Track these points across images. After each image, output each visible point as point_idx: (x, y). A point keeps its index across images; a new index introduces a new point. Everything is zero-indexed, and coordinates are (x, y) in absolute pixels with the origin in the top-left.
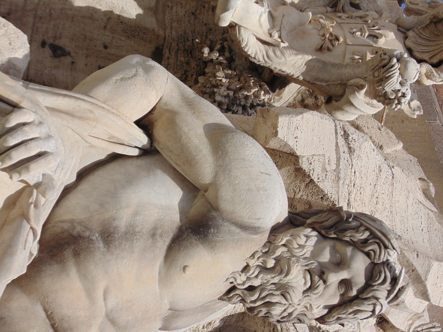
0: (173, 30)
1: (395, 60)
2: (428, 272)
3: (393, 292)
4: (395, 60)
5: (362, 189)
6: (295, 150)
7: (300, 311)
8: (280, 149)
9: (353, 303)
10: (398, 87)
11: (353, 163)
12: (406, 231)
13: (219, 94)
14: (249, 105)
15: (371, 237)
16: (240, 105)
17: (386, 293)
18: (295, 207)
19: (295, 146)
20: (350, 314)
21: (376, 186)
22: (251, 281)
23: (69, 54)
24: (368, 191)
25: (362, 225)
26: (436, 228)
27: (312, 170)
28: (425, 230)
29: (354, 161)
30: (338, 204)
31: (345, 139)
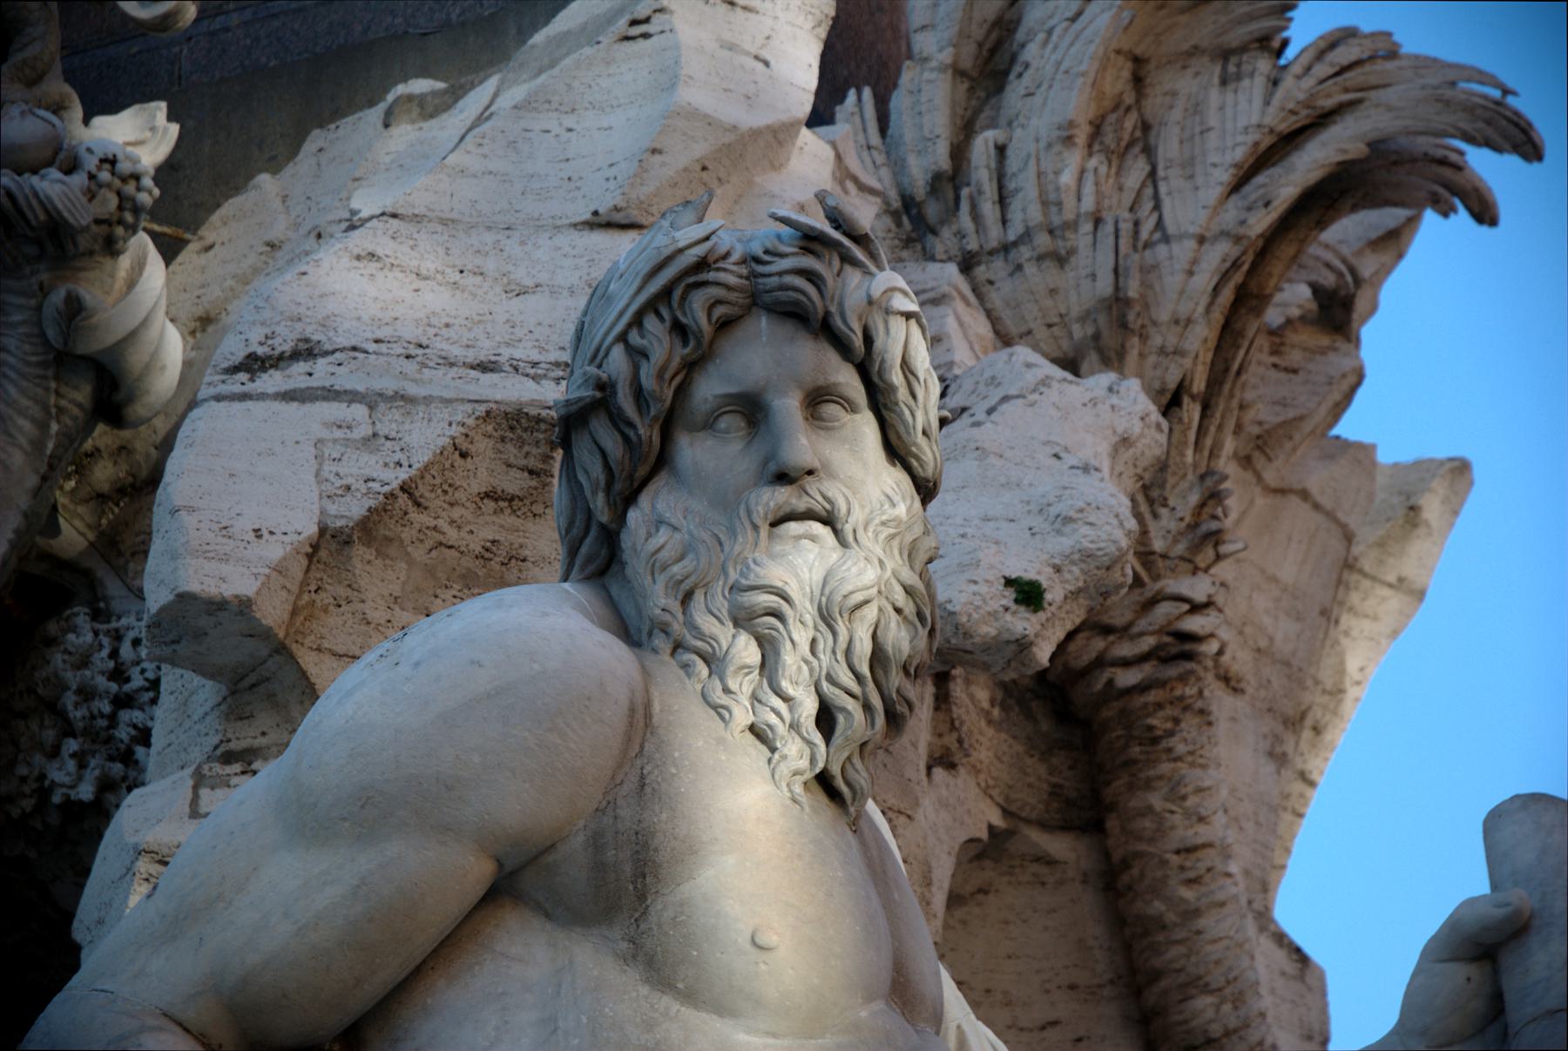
2: (710, 122)
3: (848, 249)
5: (434, 321)
6: (301, 538)
7: (900, 562)
8: (295, 588)
9: (881, 384)
11: (348, 344)
12: (572, 185)
13: (72, 787)
14: (114, 687)
15: (665, 313)
16: (113, 719)
17: (853, 277)
18: (488, 544)
20: (914, 396)
21: (424, 272)
22: (802, 720)
25: (623, 338)
27: (371, 484)
28: (569, 121)
29: (342, 341)
30: (485, 405)
31: (264, 369)
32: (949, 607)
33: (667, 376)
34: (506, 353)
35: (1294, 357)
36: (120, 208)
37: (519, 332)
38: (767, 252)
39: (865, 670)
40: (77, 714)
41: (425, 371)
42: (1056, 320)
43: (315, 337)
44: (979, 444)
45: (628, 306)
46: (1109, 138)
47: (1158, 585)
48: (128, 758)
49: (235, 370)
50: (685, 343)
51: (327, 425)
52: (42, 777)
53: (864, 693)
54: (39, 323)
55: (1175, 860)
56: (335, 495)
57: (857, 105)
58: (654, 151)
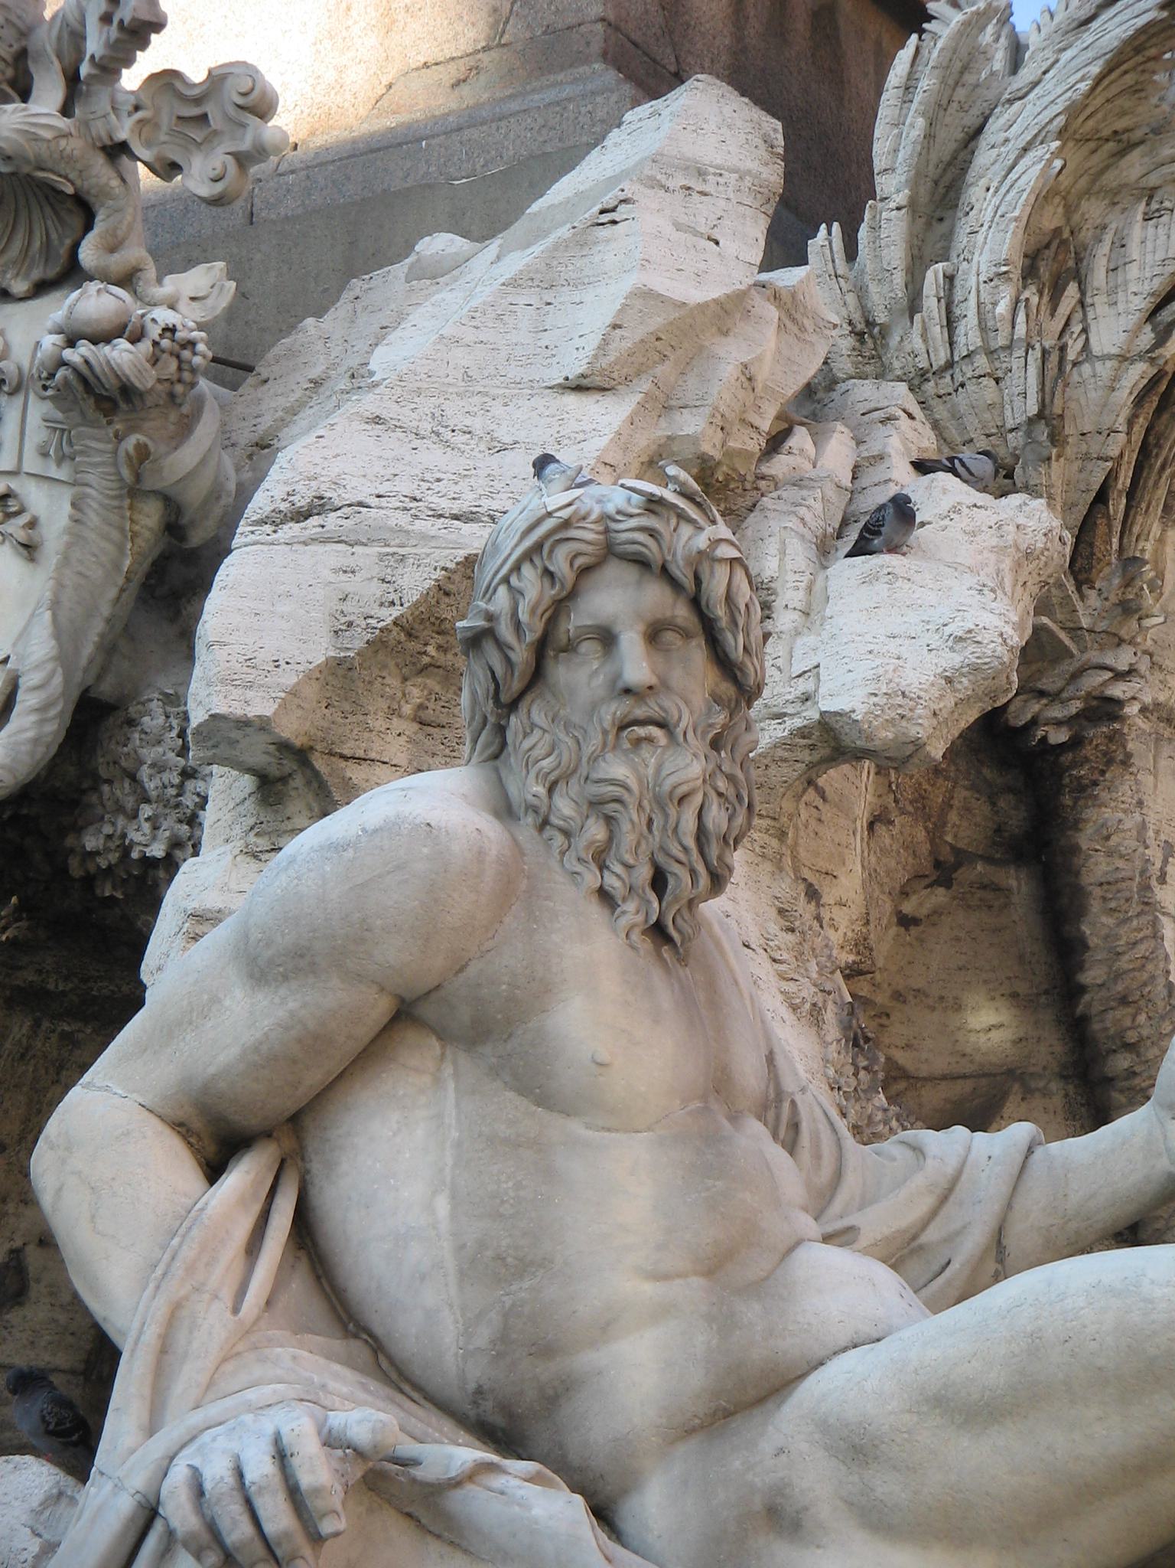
1: (69, 354)
4: (69, 354)
5: (428, 476)
6: (311, 667)
10: (145, 346)
11: (354, 499)
12: (549, 352)
13: (146, 846)
14: (181, 761)
15: (537, 561)
16: (181, 787)
17: (686, 530)
19: (301, 668)
21: (422, 432)
23: (16, 1253)
24: (433, 457)
25: (506, 580)
26: (543, 264)
27: (369, 621)
32: (853, 716)
33: (540, 611)
34: (486, 504)
36: (180, 369)
37: (497, 485)
38: (619, 512)
39: (690, 842)
40: (151, 786)
41: (417, 522)
42: (994, 431)
43: (327, 495)
44: (890, 570)
45: (510, 555)
46: (1045, 271)
47: (1085, 657)
48: (193, 821)
49: (262, 522)
50: (553, 584)
51: (335, 571)
52: (124, 836)
53: (690, 862)
54: (115, 464)
56: (340, 630)
57: (825, 241)
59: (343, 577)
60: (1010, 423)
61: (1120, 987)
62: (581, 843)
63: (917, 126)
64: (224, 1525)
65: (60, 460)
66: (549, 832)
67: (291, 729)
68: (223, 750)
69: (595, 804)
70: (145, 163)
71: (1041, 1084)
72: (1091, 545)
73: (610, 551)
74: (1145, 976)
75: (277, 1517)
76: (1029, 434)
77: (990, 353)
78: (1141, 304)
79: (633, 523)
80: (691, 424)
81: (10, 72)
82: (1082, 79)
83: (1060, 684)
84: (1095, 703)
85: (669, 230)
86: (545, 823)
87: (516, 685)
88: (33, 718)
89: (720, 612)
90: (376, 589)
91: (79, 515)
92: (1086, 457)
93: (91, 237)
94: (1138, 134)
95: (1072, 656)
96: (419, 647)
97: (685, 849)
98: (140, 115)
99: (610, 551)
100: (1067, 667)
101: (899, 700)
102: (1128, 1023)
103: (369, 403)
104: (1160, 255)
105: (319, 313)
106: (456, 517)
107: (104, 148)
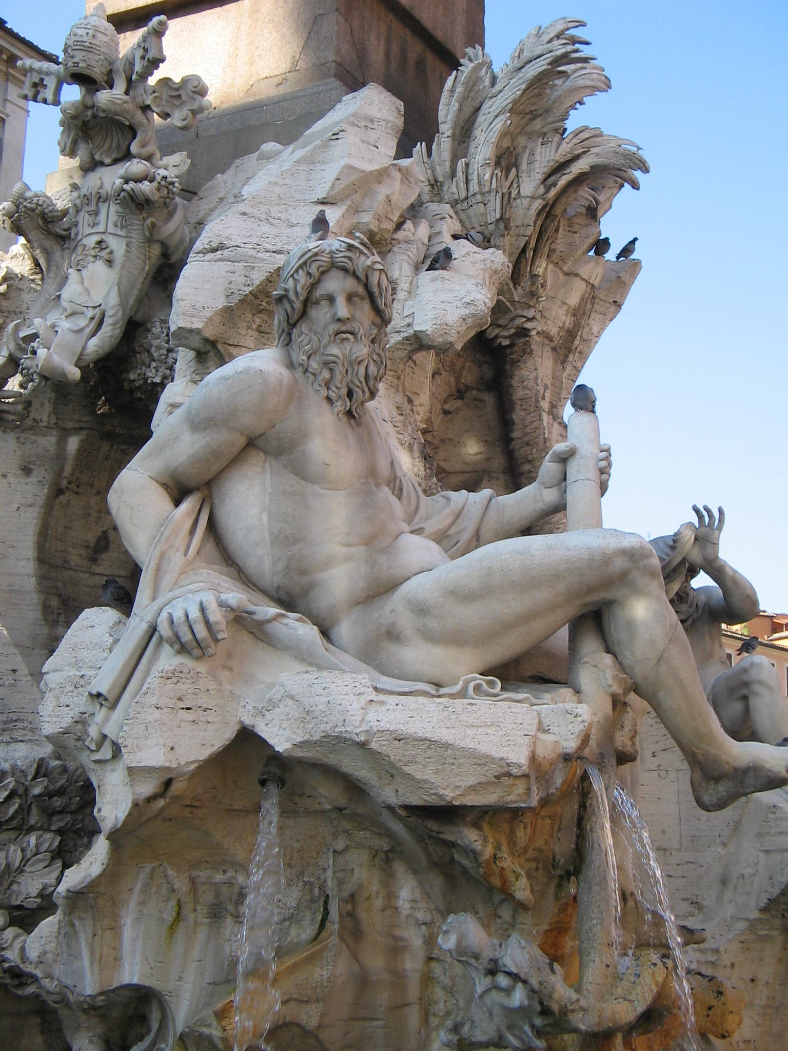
0: (83, 419)
1: (125, 187)
4: (125, 187)
5: (263, 236)
10: (155, 184)
14: (167, 346)
15: (305, 269)
16: (167, 356)
17: (363, 258)
23: (105, 532)
24: (266, 228)
25: (292, 276)
29: (233, 244)
34: (286, 247)
35: (576, 228)
36: (168, 193)
39: (363, 380)
40: (155, 355)
46: (503, 163)
47: (517, 312)
48: (171, 368)
49: (199, 253)
50: (311, 278)
52: (145, 374)
54: (143, 230)
55: (519, 402)
57: (419, 149)
58: (338, 179)
59: (231, 275)
60: (489, 222)
61: (526, 439)
62: (320, 378)
63: (455, 106)
64: (181, 634)
65: (122, 227)
66: (308, 374)
67: (209, 333)
68: (183, 342)
69: (326, 364)
70: (157, 114)
71: (495, 475)
72: (520, 269)
73: (333, 265)
74: (536, 435)
75: (201, 632)
76: (496, 226)
77: (482, 194)
78: (540, 177)
79: (342, 254)
80: (366, 218)
81: (105, 78)
82: (518, 90)
83: (506, 322)
84: (519, 330)
85: (359, 143)
86: (306, 371)
87: (296, 317)
88: (111, 328)
89: (376, 290)
90: (243, 279)
91: (128, 249)
92: (518, 235)
93: (135, 141)
94: (540, 112)
95: (511, 312)
96: (259, 303)
97: (361, 382)
98: (155, 95)
99: (333, 265)
100: (509, 316)
101: (445, 327)
102: (529, 452)
103: (241, 207)
104: (547, 158)
105: (223, 173)
106: (274, 252)
107: (141, 107)
